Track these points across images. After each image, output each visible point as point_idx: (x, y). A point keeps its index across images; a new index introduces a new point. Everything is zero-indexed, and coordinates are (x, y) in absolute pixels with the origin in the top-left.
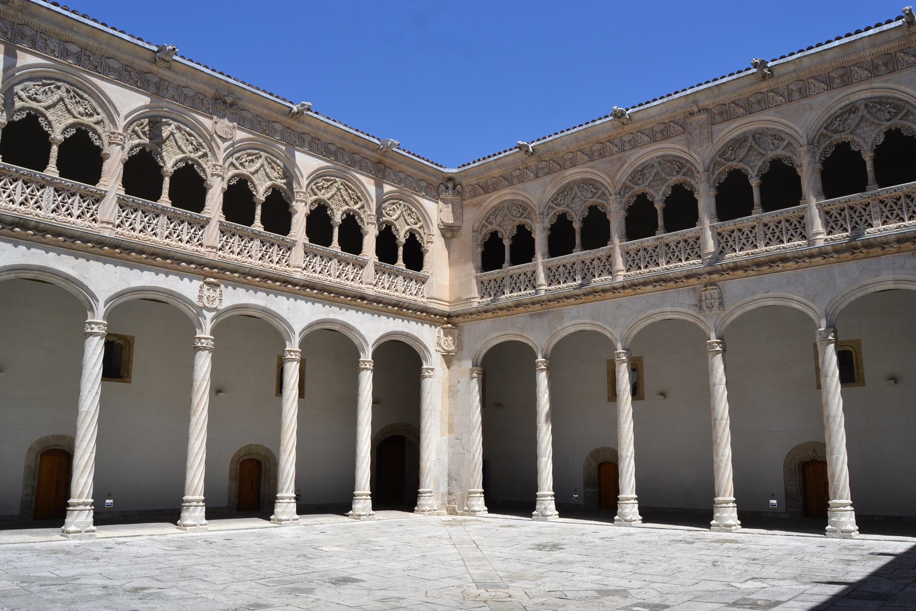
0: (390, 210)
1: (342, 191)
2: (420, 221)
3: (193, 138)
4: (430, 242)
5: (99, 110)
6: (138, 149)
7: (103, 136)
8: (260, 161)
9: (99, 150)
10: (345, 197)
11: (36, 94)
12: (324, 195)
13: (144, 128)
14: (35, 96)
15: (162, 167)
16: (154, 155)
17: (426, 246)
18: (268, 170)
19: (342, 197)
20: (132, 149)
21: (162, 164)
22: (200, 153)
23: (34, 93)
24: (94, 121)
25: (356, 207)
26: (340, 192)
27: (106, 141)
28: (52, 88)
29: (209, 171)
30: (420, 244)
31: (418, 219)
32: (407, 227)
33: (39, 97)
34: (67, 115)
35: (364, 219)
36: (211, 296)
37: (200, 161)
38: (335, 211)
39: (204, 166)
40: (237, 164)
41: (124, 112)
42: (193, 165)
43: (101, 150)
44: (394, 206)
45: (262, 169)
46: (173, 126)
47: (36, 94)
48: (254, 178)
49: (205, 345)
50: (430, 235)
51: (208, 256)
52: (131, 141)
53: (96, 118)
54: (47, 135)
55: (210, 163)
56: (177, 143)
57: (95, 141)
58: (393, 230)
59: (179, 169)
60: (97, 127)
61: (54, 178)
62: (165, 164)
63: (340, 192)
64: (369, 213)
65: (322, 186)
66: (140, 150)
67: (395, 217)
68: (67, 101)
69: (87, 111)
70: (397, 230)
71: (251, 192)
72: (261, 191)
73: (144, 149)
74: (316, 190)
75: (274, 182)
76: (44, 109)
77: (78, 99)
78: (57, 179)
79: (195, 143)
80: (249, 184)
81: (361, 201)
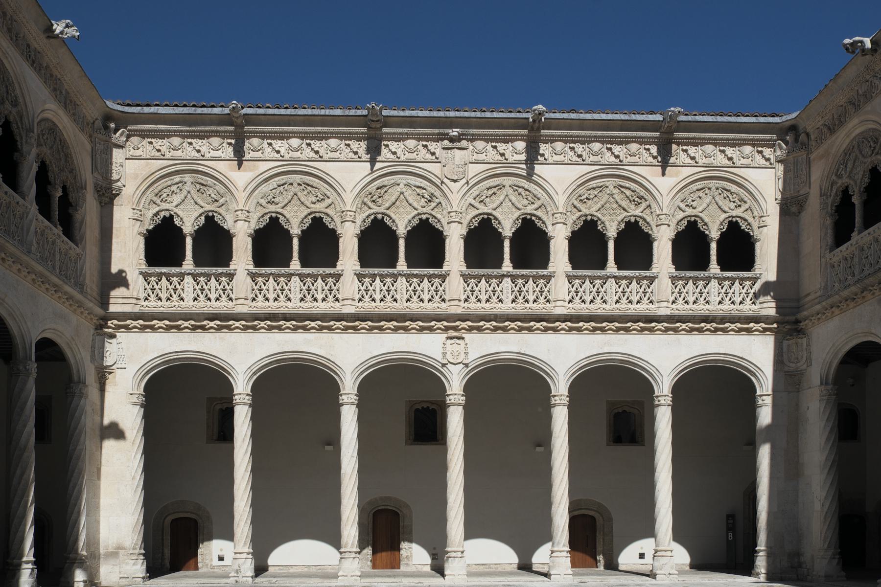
0: (693, 201)
1: (615, 196)
2: (745, 202)
3: (424, 191)
4: (762, 227)
5: (329, 194)
6: (370, 220)
7: (335, 218)
8: (504, 192)
9: (334, 231)
10: (620, 202)
11: (274, 198)
12: (591, 209)
13: (372, 197)
14: (273, 200)
15: (396, 230)
16: (386, 221)
17: (756, 233)
18: (514, 199)
19: (617, 202)
20: (364, 221)
21: (395, 228)
22: (433, 205)
23: (271, 197)
24: (326, 206)
25: (637, 212)
26: (614, 198)
27: (338, 220)
28: (286, 188)
29: (444, 221)
30: (748, 233)
31: (742, 200)
32: (724, 216)
33: (276, 200)
34: (303, 208)
35: (652, 223)
36: (455, 351)
37: (434, 213)
38: (607, 223)
39: (439, 216)
40: (477, 204)
41: (349, 187)
42: (428, 219)
43: (335, 231)
44: (701, 193)
45: (507, 200)
46: (402, 186)
47: (274, 198)
48: (496, 214)
49: (452, 401)
50: (761, 217)
51: (450, 310)
52: (362, 215)
53: (328, 202)
54: (288, 231)
55: (445, 212)
56: (407, 202)
57: (329, 225)
58: (700, 225)
59: (414, 228)
60: (328, 211)
61: (297, 270)
62: (397, 227)
63: (614, 198)
64: (658, 213)
65: (587, 198)
66: (372, 220)
67: (700, 209)
68: (299, 194)
69: (318, 198)
70: (706, 224)
71: (496, 230)
72: (507, 227)
73: (375, 217)
74: (578, 205)
75: (522, 211)
76: (281, 210)
77: (309, 188)
78: (299, 270)
79: (426, 196)
80: (493, 222)
81: (646, 201)
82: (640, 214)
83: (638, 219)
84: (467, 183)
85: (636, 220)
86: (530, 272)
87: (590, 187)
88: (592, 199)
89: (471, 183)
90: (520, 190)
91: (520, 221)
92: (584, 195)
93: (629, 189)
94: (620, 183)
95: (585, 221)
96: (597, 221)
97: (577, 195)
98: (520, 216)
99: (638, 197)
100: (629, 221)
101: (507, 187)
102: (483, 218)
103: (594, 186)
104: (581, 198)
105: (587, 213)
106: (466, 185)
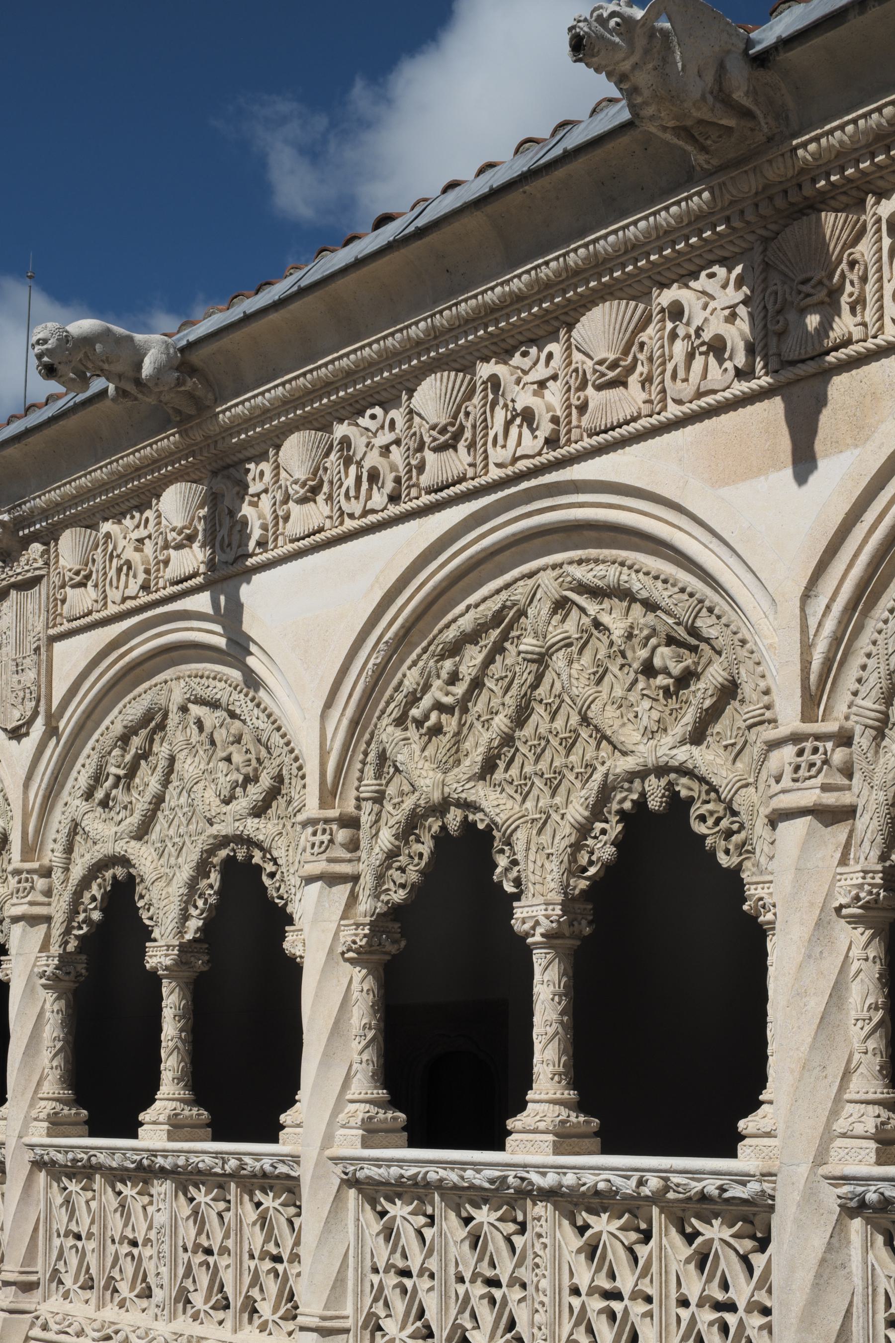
82: (682, 754)
83: (684, 787)
84: (52, 731)
85: (673, 796)
86: (217, 1154)
87: (451, 634)
88: (463, 705)
89: (67, 725)
90: (210, 718)
91: (214, 878)
92: (427, 687)
93: (625, 595)
94: (579, 573)
95: (442, 839)
96: (489, 829)
97: (399, 697)
98: (211, 852)
99: (671, 641)
100: (641, 804)
101: (174, 718)
102: (114, 877)
103: (466, 623)
104: (415, 712)
105: (436, 796)
106: (54, 740)
